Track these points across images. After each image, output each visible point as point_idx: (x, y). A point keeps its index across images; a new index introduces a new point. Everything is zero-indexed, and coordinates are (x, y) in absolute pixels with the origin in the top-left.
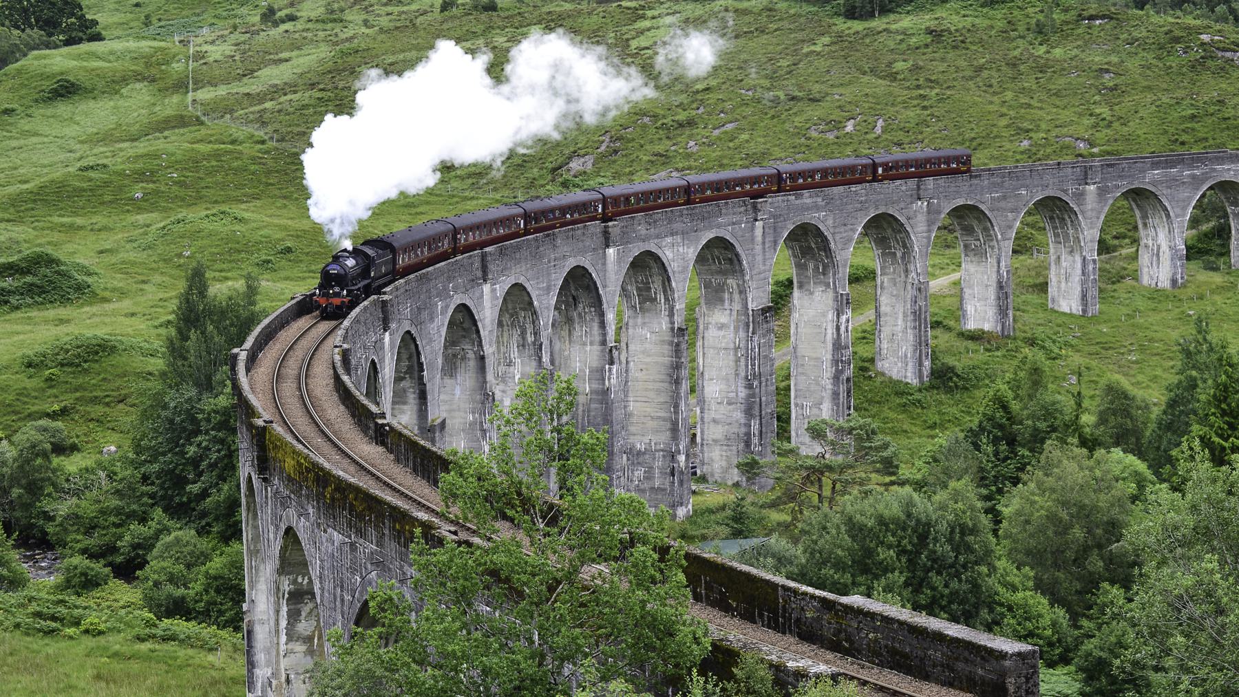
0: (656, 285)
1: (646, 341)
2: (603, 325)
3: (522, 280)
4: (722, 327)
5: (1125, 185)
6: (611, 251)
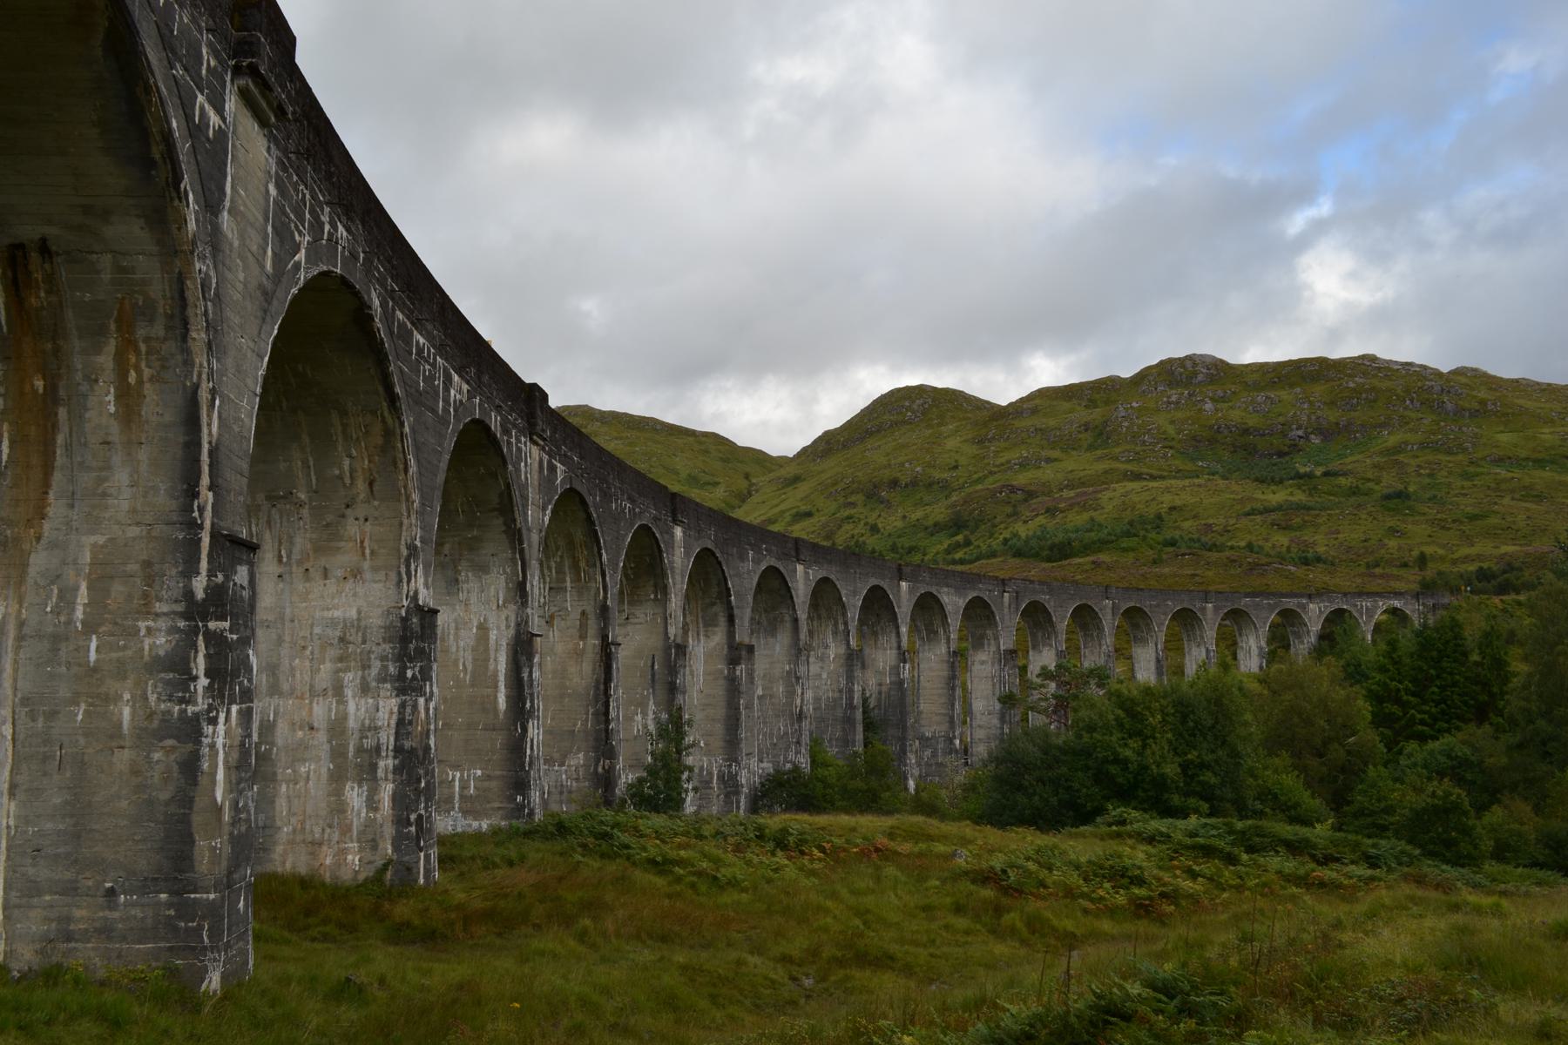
0: (937, 622)
1: (932, 661)
2: (898, 634)
3: (832, 577)
4: (983, 663)
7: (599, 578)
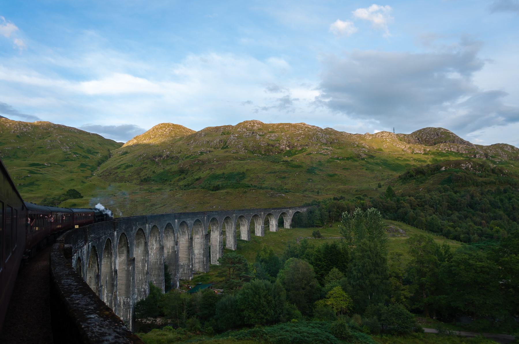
1: (183, 241)
3: (156, 225)
4: (198, 238)
5: (268, 213)
7: (96, 266)
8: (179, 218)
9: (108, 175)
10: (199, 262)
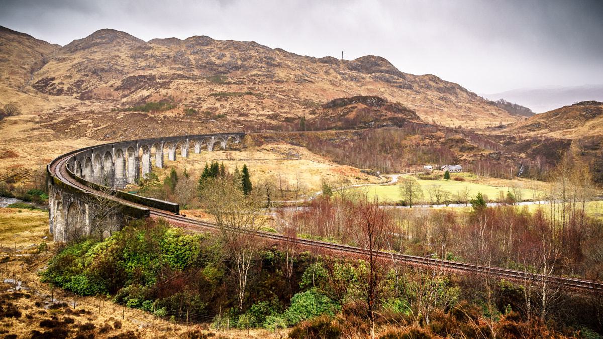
0: (121, 154)
1: (119, 163)
6: (113, 149)
8: (116, 147)
9: (44, 86)
10: (132, 177)
